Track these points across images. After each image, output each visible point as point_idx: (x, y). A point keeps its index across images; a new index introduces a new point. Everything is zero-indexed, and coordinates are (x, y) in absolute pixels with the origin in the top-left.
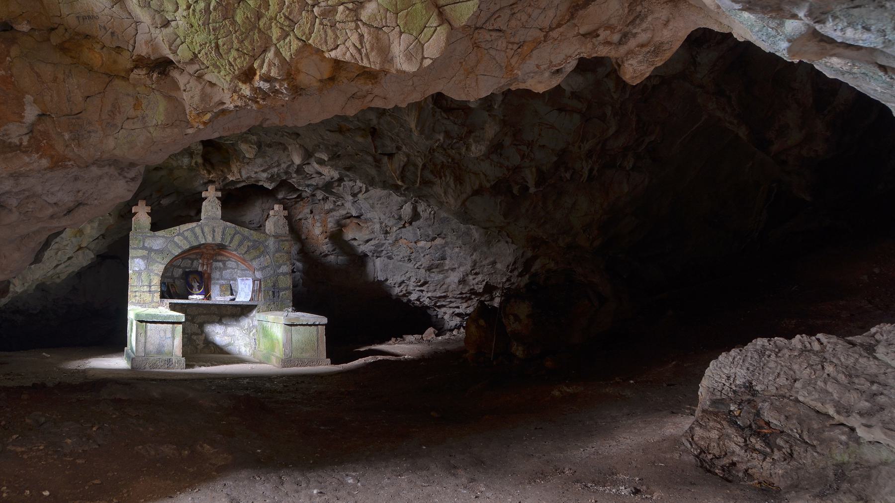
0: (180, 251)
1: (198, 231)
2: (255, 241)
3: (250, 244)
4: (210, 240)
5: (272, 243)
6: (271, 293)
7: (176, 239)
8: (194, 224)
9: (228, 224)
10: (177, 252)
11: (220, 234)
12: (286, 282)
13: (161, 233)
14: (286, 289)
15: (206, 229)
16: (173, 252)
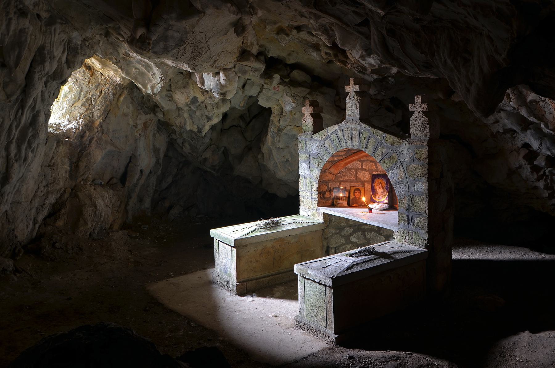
0: (329, 156)
1: (340, 134)
2: (387, 147)
3: (384, 150)
4: (349, 146)
5: (405, 151)
6: (405, 217)
7: (326, 143)
8: (336, 127)
9: (363, 124)
10: (327, 158)
11: (357, 138)
12: (422, 204)
13: (316, 136)
14: (420, 215)
15: (346, 133)
16: (325, 157)
